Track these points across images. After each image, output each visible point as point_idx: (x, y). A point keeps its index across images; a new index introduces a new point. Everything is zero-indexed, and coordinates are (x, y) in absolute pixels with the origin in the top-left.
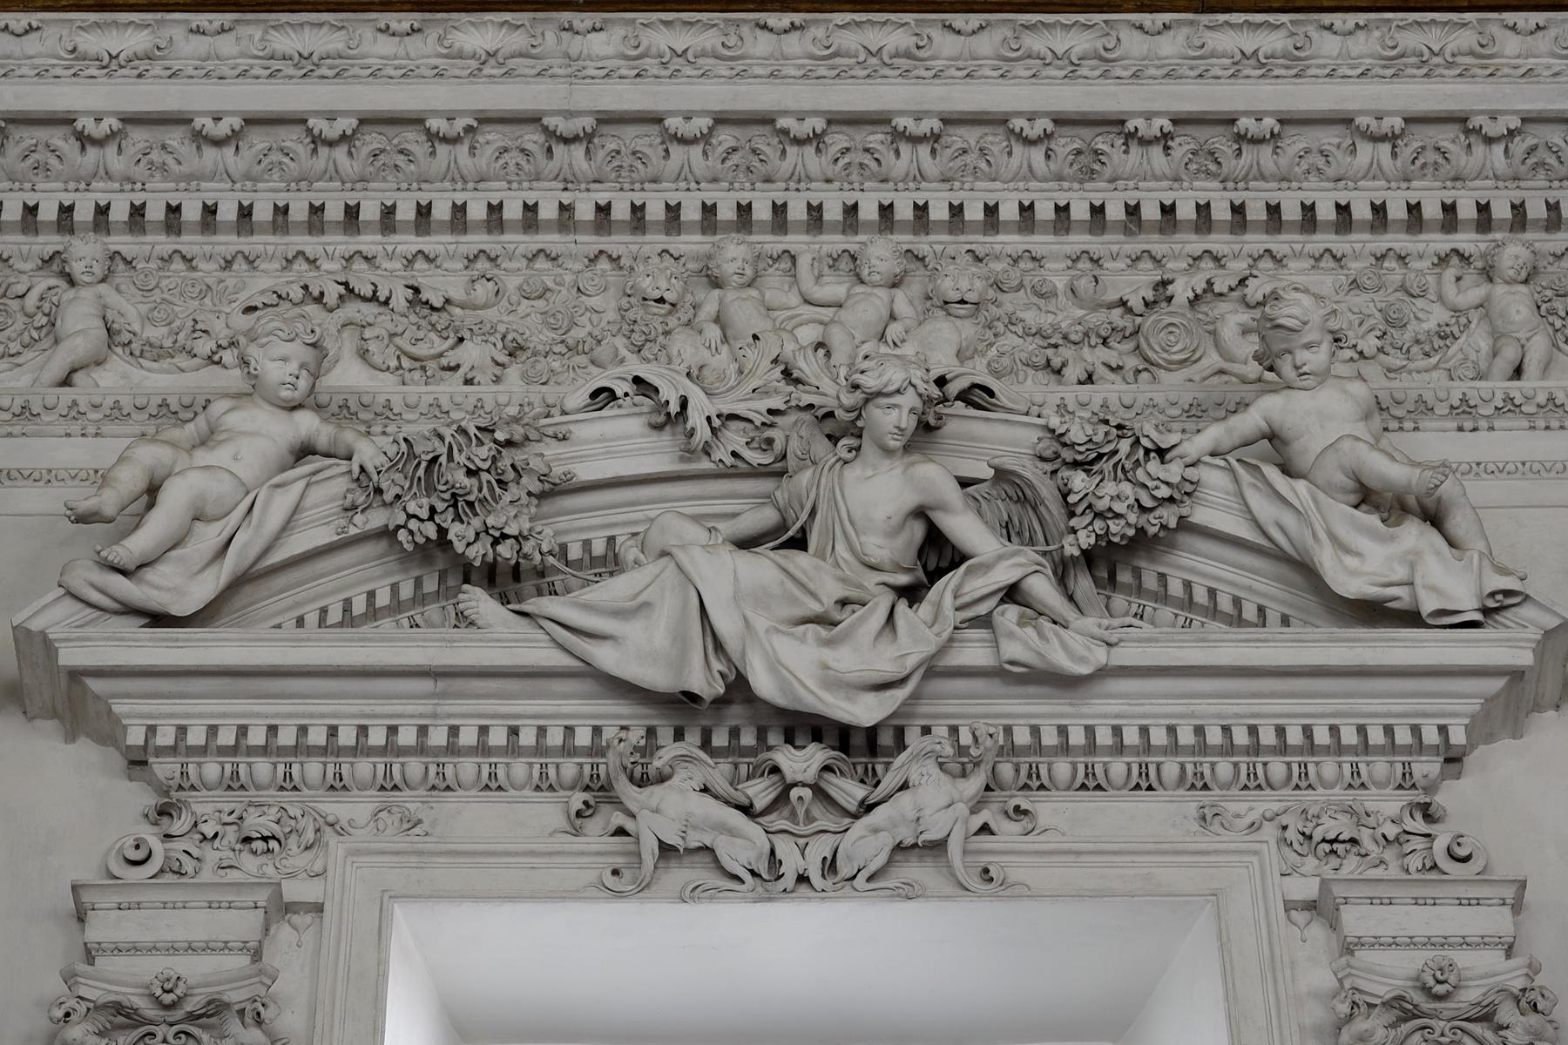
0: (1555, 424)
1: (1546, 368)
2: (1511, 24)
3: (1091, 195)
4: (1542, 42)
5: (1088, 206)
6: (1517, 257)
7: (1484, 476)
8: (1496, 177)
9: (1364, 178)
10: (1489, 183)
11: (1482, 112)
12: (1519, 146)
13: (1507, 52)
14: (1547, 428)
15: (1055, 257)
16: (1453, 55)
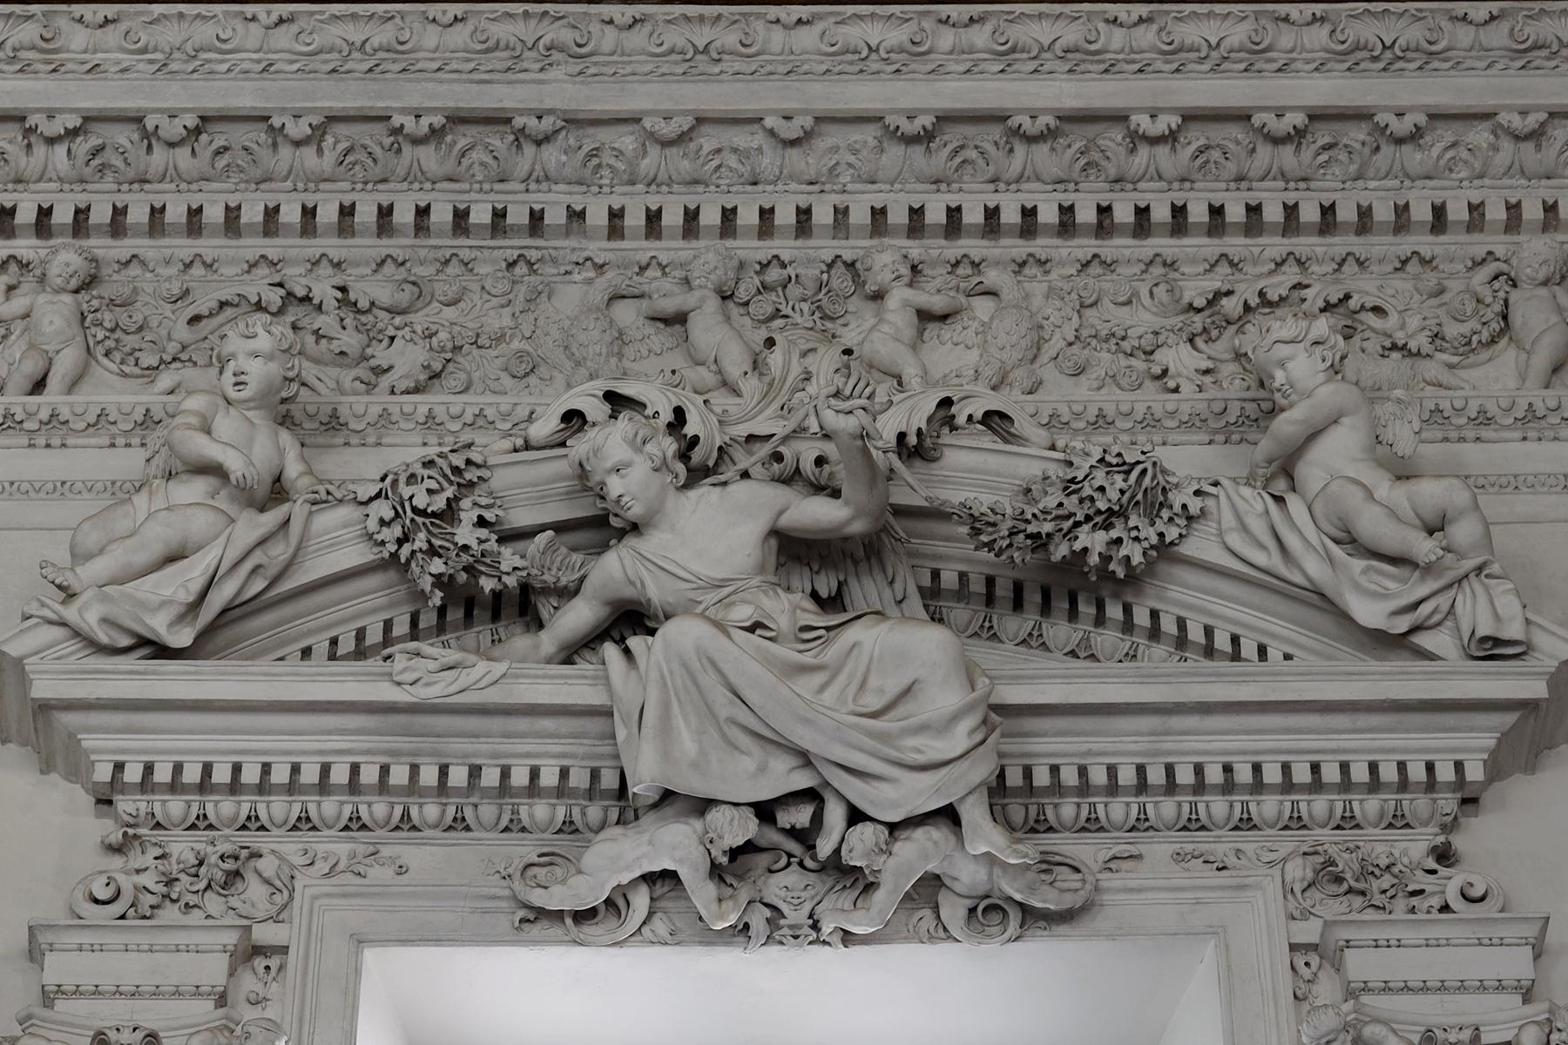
0: (56, 441)
1: (73, 385)
2: (77, 16)
3: (151, 197)
4: (112, 35)
5: (451, 208)
6: (67, 265)
7: (18, 496)
8: (60, 179)
9: (39, 180)
10: (53, 186)
11: (38, 110)
12: (83, 146)
13: (73, 47)
14: (48, 446)
15: (232, 262)
16: (14, 49)
